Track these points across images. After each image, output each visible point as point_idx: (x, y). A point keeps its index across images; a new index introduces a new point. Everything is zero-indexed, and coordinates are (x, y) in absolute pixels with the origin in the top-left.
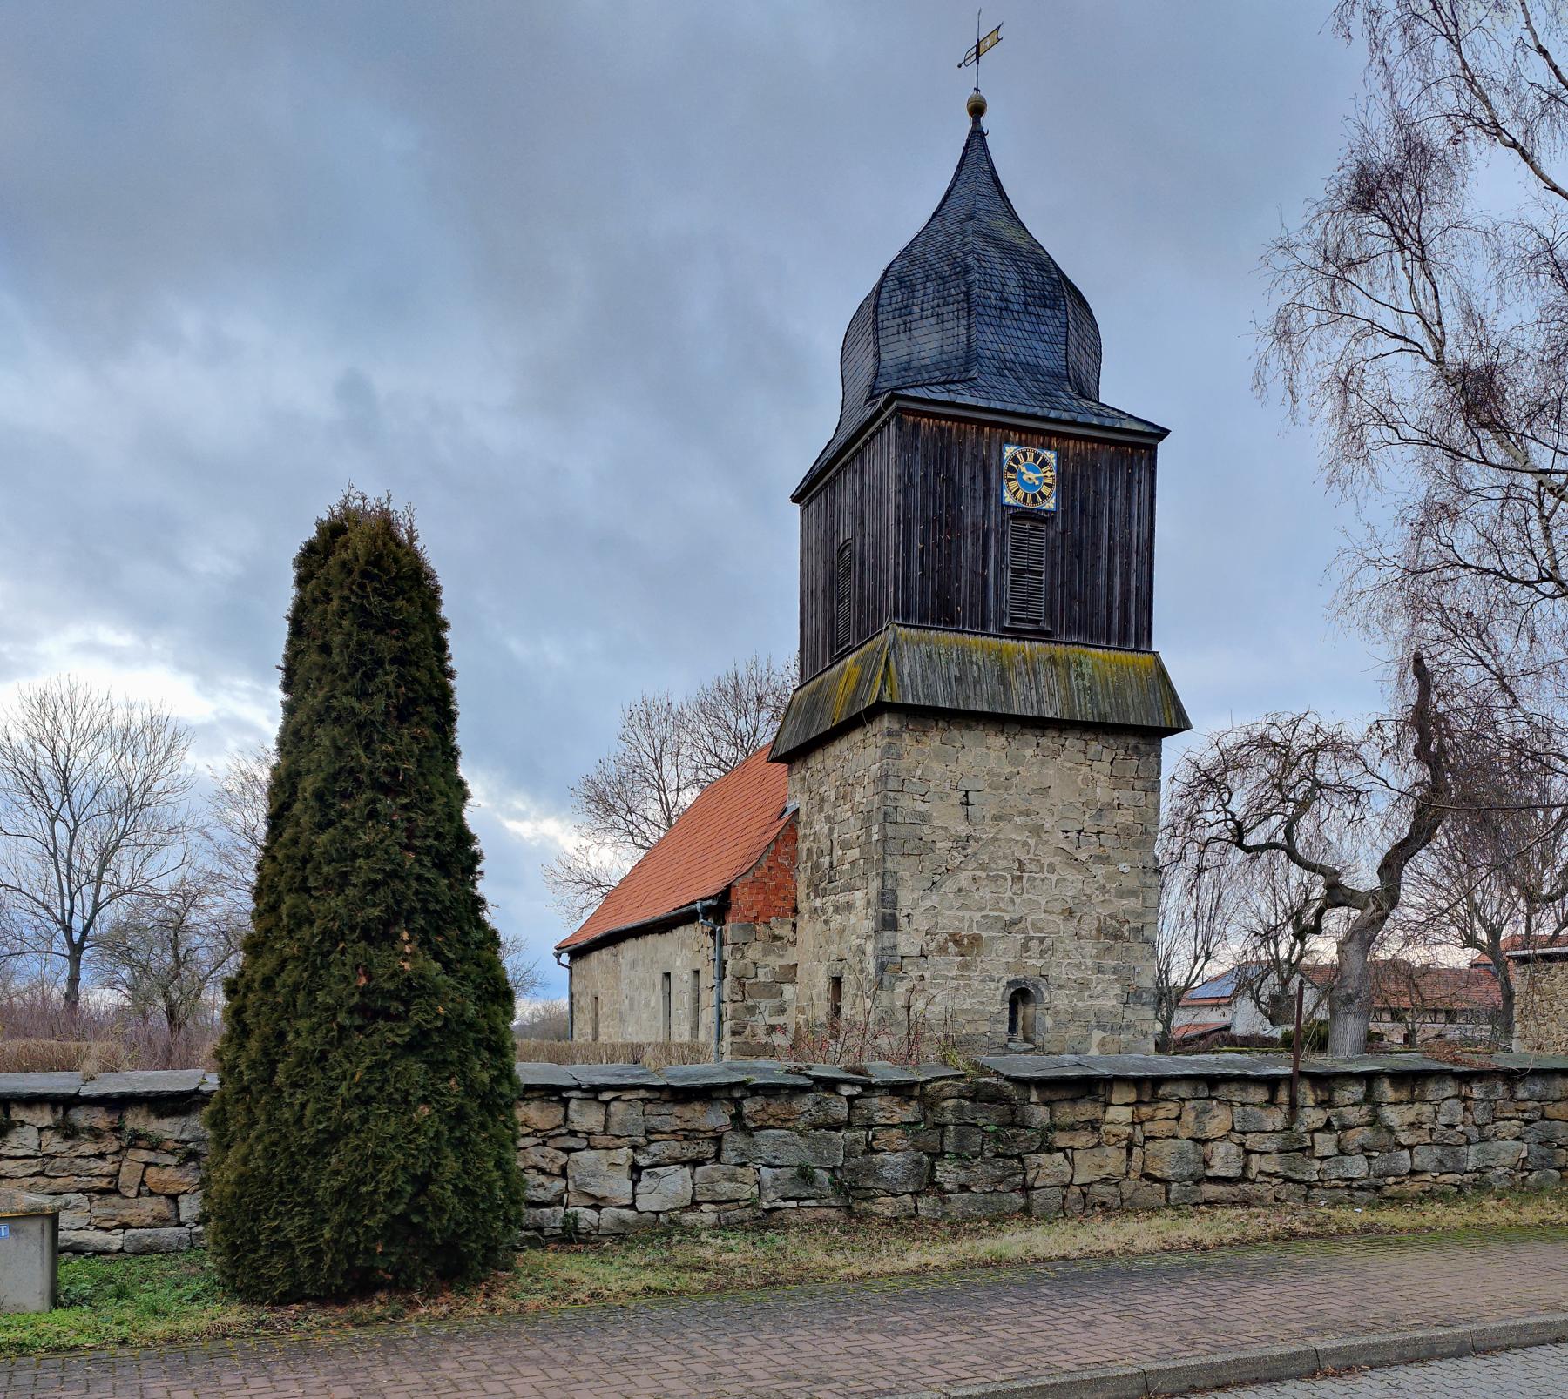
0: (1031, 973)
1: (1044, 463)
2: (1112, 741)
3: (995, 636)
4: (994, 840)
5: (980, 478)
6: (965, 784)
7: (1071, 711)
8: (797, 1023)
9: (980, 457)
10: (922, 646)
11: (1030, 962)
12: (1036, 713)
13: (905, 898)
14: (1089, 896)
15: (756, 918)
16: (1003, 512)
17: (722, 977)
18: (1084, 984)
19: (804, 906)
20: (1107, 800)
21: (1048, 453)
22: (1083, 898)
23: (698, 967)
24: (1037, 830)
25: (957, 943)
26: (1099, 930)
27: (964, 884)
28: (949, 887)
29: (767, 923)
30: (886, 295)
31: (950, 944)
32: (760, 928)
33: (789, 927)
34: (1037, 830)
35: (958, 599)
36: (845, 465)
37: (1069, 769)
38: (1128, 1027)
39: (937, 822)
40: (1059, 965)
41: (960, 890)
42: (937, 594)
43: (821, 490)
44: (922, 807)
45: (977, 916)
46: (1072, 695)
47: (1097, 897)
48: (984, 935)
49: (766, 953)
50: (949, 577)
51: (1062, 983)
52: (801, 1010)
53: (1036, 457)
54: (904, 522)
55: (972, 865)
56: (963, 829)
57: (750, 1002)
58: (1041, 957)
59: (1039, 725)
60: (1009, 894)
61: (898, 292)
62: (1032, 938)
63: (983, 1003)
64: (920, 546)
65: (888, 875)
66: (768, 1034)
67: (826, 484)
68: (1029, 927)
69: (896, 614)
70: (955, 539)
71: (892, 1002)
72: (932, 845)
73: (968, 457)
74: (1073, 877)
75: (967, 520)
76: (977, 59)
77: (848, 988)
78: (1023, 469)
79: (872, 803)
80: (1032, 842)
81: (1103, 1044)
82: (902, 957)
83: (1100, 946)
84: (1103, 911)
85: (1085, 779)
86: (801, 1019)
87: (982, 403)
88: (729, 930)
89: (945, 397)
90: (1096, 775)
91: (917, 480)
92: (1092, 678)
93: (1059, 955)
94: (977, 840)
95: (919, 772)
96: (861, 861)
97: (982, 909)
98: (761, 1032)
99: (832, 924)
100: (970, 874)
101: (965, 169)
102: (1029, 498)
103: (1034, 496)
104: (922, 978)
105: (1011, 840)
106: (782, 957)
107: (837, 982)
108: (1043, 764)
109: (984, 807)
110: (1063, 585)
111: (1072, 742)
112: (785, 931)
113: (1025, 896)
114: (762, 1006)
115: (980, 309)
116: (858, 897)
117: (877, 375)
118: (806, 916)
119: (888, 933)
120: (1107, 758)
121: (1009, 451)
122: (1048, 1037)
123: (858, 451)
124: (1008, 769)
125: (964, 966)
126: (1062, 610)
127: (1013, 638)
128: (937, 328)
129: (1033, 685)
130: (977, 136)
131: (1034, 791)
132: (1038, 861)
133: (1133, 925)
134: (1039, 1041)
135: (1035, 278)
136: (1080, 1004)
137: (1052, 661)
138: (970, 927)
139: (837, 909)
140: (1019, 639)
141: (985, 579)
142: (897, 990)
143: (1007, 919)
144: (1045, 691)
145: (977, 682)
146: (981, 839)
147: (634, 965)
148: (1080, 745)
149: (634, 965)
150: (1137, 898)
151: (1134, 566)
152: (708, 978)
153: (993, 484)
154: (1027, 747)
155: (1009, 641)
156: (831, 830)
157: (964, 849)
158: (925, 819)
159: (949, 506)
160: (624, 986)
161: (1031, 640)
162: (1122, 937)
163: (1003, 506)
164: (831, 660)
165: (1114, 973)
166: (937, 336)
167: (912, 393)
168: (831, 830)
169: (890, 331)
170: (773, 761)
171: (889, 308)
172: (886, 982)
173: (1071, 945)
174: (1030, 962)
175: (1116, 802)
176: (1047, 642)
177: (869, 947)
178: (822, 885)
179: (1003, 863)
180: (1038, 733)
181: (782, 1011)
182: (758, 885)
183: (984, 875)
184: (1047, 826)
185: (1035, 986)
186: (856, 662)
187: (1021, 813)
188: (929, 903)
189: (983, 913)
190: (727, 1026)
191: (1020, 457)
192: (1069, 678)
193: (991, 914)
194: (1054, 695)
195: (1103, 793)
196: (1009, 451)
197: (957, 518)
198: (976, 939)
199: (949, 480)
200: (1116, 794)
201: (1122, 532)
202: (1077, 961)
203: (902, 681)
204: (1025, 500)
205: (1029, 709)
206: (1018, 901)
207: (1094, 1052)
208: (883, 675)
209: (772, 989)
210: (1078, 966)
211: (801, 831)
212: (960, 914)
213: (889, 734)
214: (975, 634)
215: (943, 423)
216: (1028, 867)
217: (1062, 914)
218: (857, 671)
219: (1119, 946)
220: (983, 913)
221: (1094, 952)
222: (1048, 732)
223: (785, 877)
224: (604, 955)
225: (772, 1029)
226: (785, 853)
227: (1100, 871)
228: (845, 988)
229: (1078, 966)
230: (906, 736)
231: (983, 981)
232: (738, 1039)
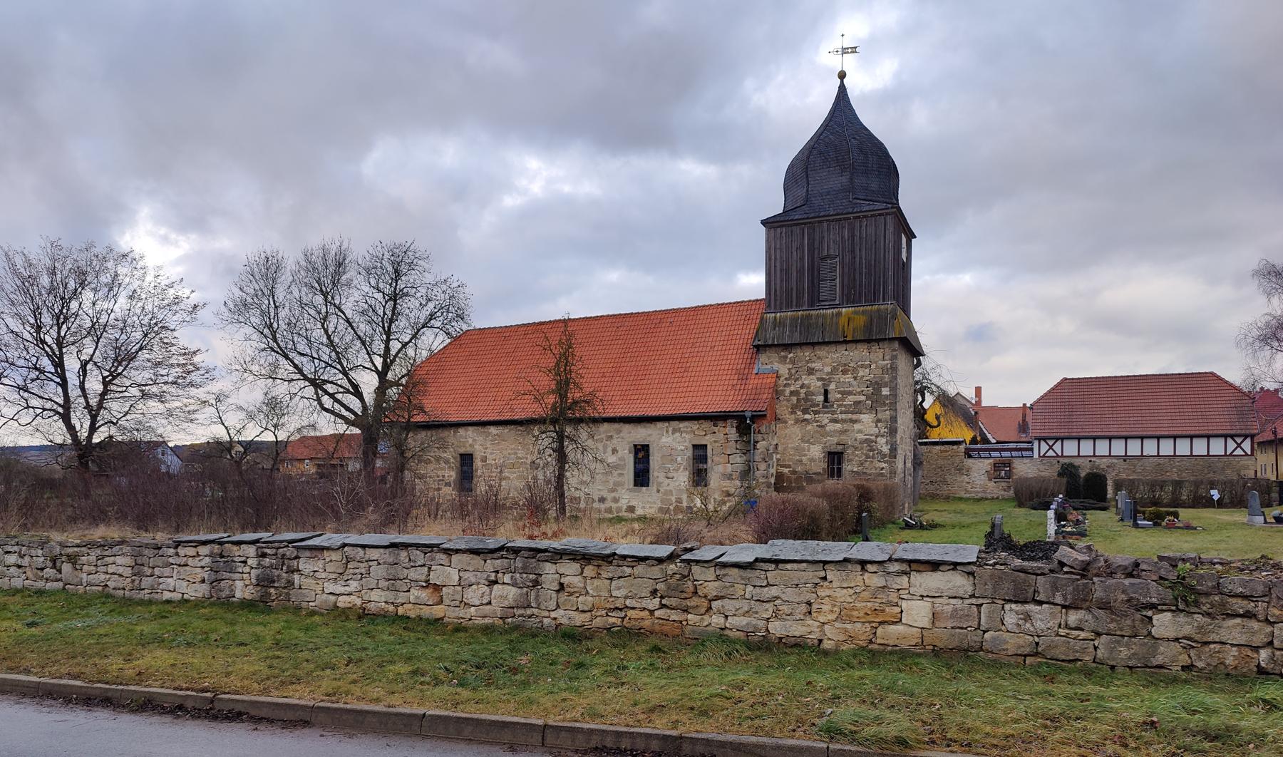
52: (789, 466)
139: (836, 421)
177: (882, 441)
186: (855, 313)
211: (782, 381)
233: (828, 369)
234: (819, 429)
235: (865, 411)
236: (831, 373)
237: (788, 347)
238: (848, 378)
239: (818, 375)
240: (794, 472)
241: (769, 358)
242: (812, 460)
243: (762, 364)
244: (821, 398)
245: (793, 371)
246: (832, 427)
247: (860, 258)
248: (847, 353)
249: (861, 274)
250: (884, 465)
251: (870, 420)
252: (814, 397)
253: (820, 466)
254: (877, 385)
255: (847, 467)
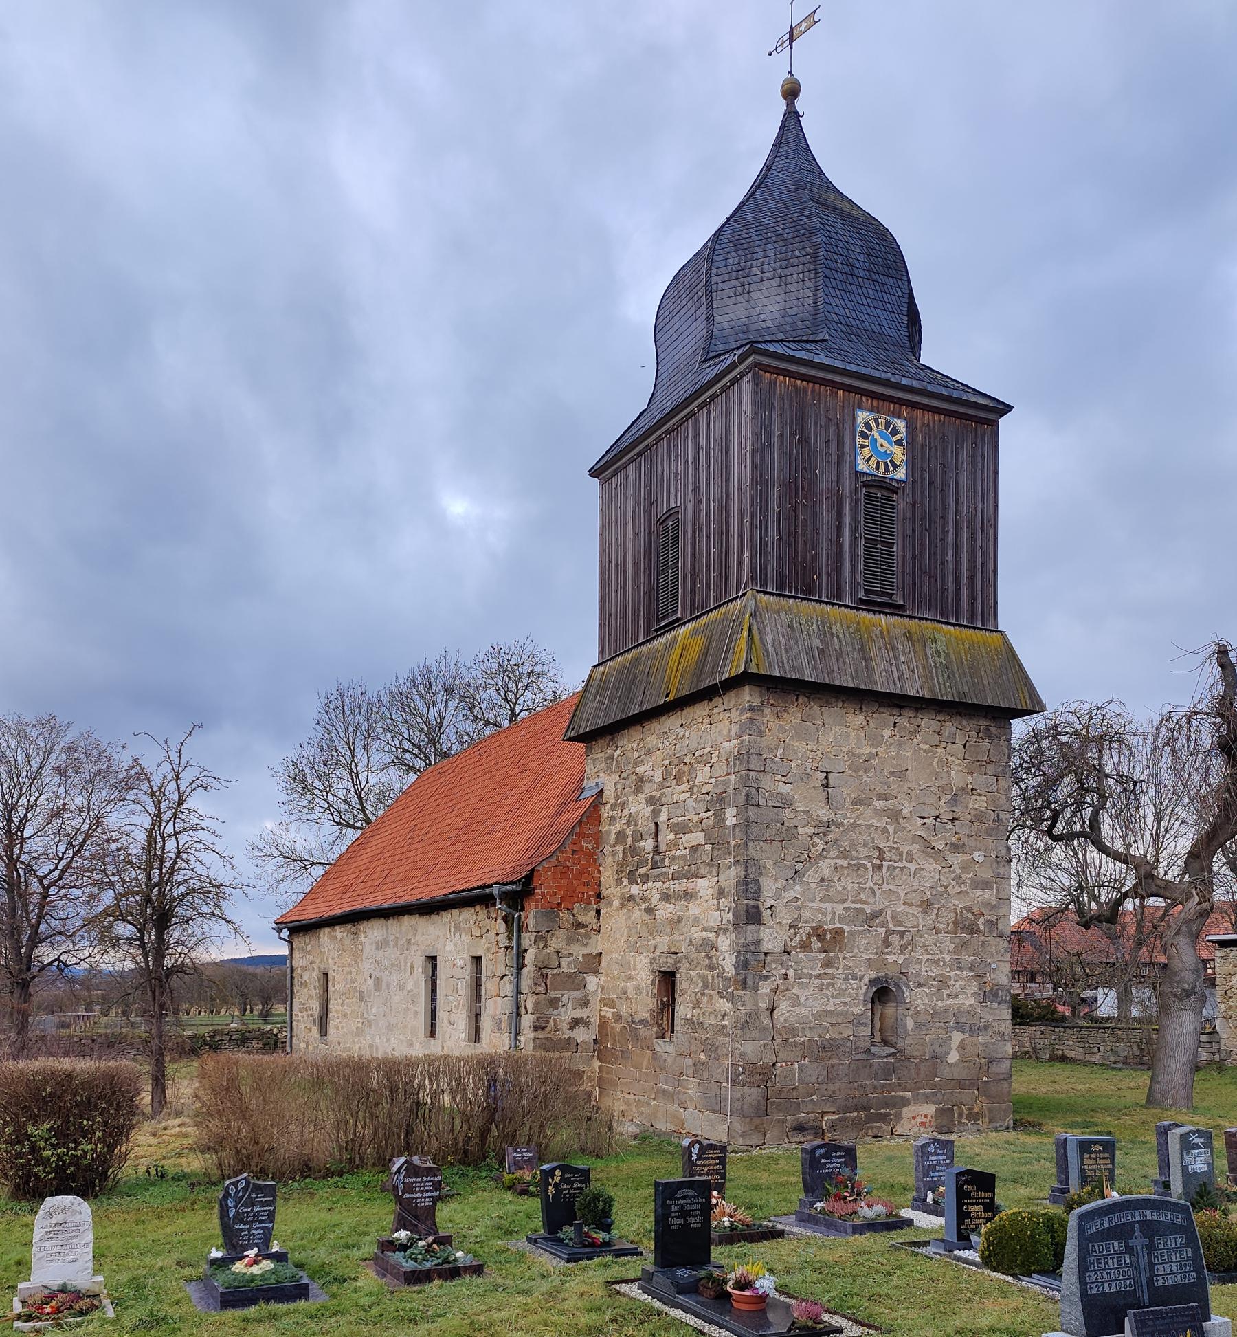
0: (892, 971)
1: (895, 432)
2: (965, 723)
3: (852, 608)
4: (855, 825)
5: (835, 442)
6: (825, 765)
7: (933, 692)
8: (602, 1017)
9: (835, 421)
10: (783, 615)
11: (892, 958)
12: (898, 691)
13: (769, 888)
14: (946, 887)
15: (559, 904)
16: (857, 478)
17: (521, 966)
18: (943, 982)
19: (611, 890)
20: (961, 785)
21: (898, 421)
22: (941, 889)
23: (479, 954)
24: (895, 816)
25: (820, 938)
26: (956, 923)
27: (826, 873)
28: (811, 877)
29: (570, 910)
30: (721, 257)
31: (813, 939)
32: (564, 914)
33: (593, 914)
34: (895, 816)
35: (814, 568)
36: (667, 432)
37: (925, 751)
38: (986, 1027)
39: (800, 806)
40: (919, 961)
41: (822, 880)
42: (794, 561)
43: (631, 461)
44: (785, 789)
45: (839, 908)
46: (931, 673)
47: (954, 889)
48: (846, 928)
49: (571, 941)
50: (806, 543)
51: (922, 981)
52: (610, 1004)
53: (888, 424)
54: (761, 482)
55: (834, 853)
56: (824, 813)
57: (553, 995)
58: (902, 953)
59: (897, 702)
60: (870, 884)
61: (734, 254)
62: (892, 932)
63: (845, 1004)
64: (777, 510)
65: (751, 863)
66: (571, 1028)
67: (640, 454)
68: (889, 919)
69: (753, 579)
70: (810, 504)
71: (757, 1005)
72: (792, 830)
73: (823, 421)
74: (930, 865)
75: (821, 485)
76: (791, 44)
77: (687, 984)
78: (877, 435)
79: (726, 783)
80: (891, 828)
81: (962, 1046)
82: (766, 954)
83: (957, 941)
84: (960, 903)
85: (940, 761)
86: (609, 1013)
87: (838, 364)
88: (530, 917)
89: (801, 355)
90: (950, 758)
91: (774, 440)
92: (947, 655)
93: (919, 950)
94: (838, 825)
95: (780, 751)
96: (708, 847)
97: (843, 901)
98: (564, 1026)
99: (659, 914)
100: (832, 862)
101: (783, 148)
102: (882, 466)
103: (886, 464)
104: (786, 976)
105: (871, 826)
106: (586, 945)
107: (667, 979)
108: (900, 745)
109: (845, 791)
110: (914, 558)
111: (928, 722)
112: (588, 918)
113: (885, 887)
114: (564, 999)
115: (828, 272)
116: (704, 886)
117: (710, 338)
118: (616, 903)
119: (751, 927)
120: (961, 740)
121: (862, 416)
122: (909, 1040)
123: (692, 414)
124: (867, 750)
125: (828, 964)
126: (914, 584)
127: (869, 611)
128: (780, 290)
129: (893, 661)
130: (792, 118)
131: (891, 773)
132: (897, 849)
133: (988, 917)
134: (900, 1045)
135: (877, 247)
136: (940, 1004)
137: (908, 636)
138: (833, 920)
139: (666, 897)
140: (875, 612)
141: (840, 547)
142: (761, 991)
143: (868, 911)
144: (904, 667)
145: (839, 655)
146: (842, 824)
147: (381, 945)
148: (935, 725)
149: (381, 945)
150: (991, 889)
151: (979, 543)
152: (496, 964)
153: (847, 450)
154: (886, 725)
155: (865, 614)
156: (656, 813)
157: (825, 835)
158: (786, 802)
159: (805, 468)
160: (367, 965)
161: (886, 614)
162: (978, 931)
163: (857, 472)
164: (648, 632)
165: (971, 970)
166: (778, 298)
167: (771, 348)
168: (656, 813)
169: (726, 293)
170: (570, 739)
171: (724, 270)
172: (750, 982)
173: (930, 940)
174: (892, 958)
175: (970, 787)
176: (902, 616)
177: (724, 942)
178: (641, 871)
179: (864, 851)
180: (895, 711)
181: (585, 1003)
182: (562, 870)
183: (845, 864)
184: (906, 812)
185: (897, 986)
186: (694, 633)
187: (879, 797)
188: (791, 894)
189: (846, 905)
190: (527, 1020)
191: (872, 423)
192: (926, 655)
193: (853, 906)
194: (913, 672)
195: (957, 777)
196: (862, 416)
197: (812, 483)
198: (838, 933)
199: (804, 441)
200: (969, 779)
201: (968, 506)
202: (936, 957)
203: (767, 650)
204: (877, 468)
205: (892, 686)
206: (878, 892)
207: (953, 1057)
208: (747, 644)
209: (575, 981)
210: (936, 962)
211: (606, 813)
212: (823, 906)
213: (751, 709)
214: (833, 604)
215: (799, 382)
216: (887, 856)
217: (919, 906)
218: (698, 643)
219: (976, 940)
220: (846, 905)
221: (951, 947)
222: (904, 712)
223: (588, 861)
224: (339, 932)
225: (576, 1023)
226: (589, 835)
227: (956, 860)
228: (681, 984)
229: (936, 962)
230: (767, 711)
231: (846, 979)
232: (541, 1035)
233: (658, 776)
234: (646, 917)
235: (703, 870)
236: (662, 786)
237: (611, 731)
238: (679, 792)
239: (649, 790)
240: (618, 1018)
241: (594, 761)
242: (638, 990)
243: (588, 778)
244: (649, 845)
245: (620, 787)
246: (666, 911)
247: (708, 499)
248: (680, 731)
249: (708, 537)
250: (727, 1006)
251: (710, 891)
252: (642, 843)
253: (644, 1005)
254: (717, 802)
255: (683, 1009)
